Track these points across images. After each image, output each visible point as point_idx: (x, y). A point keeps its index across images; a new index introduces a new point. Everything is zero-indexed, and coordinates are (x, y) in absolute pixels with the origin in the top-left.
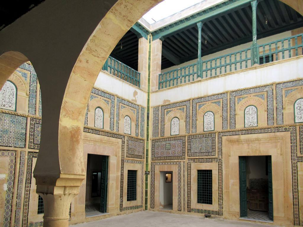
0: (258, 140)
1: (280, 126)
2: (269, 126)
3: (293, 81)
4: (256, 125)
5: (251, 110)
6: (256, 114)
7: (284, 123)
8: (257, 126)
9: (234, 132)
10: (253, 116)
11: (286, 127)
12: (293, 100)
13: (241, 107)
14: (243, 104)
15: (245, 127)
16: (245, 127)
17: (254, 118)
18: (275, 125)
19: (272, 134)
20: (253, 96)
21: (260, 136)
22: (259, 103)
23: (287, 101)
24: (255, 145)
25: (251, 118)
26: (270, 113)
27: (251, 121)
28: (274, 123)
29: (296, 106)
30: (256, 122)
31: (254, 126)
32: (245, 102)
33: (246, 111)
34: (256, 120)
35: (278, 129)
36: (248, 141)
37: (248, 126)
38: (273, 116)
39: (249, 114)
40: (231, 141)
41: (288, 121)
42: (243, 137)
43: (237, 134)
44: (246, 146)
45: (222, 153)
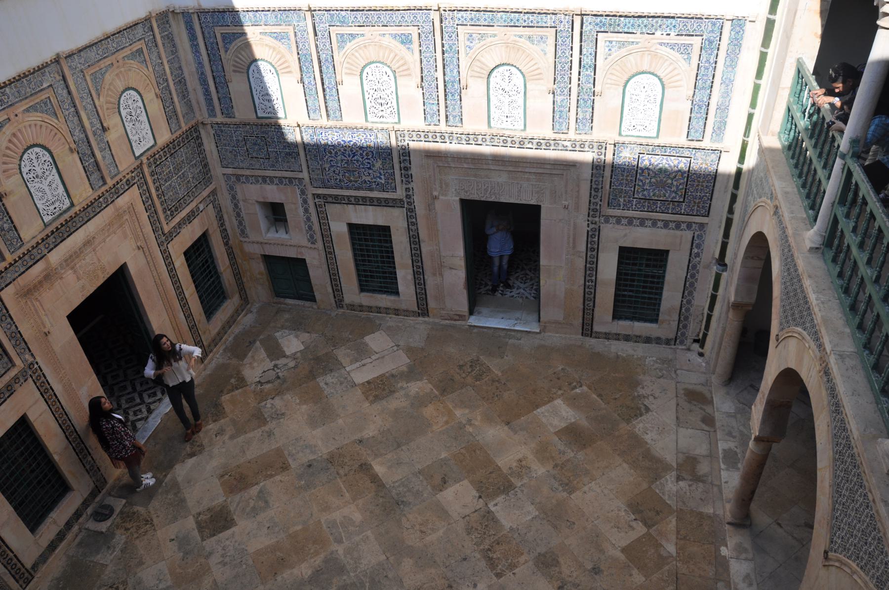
0: (88, 243)
1: (117, 179)
2: (99, 193)
3: (96, 43)
4: (67, 203)
5: (36, 164)
6: (54, 170)
7: (121, 169)
8: (72, 205)
9: (26, 257)
10: (49, 179)
11: (127, 177)
12: (112, 100)
13: (4, 163)
14: (8, 148)
15: (46, 225)
16: (46, 225)
17: (54, 186)
18: (110, 183)
19: (109, 211)
20: (27, 110)
21: (91, 227)
22: (49, 131)
23: (105, 107)
24: (88, 259)
25: (47, 189)
26: (84, 154)
27: (50, 197)
28: (103, 178)
29: (124, 113)
30: (65, 194)
31: (65, 207)
32: (10, 141)
33: (25, 170)
34: (61, 189)
35: (116, 192)
36: (70, 261)
37: (50, 217)
38: (92, 160)
39: (37, 176)
40: (28, 293)
41: (125, 164)
42: (55, 257)
43: (39, 257)
44: (69, 275)
45: (26, 343)
